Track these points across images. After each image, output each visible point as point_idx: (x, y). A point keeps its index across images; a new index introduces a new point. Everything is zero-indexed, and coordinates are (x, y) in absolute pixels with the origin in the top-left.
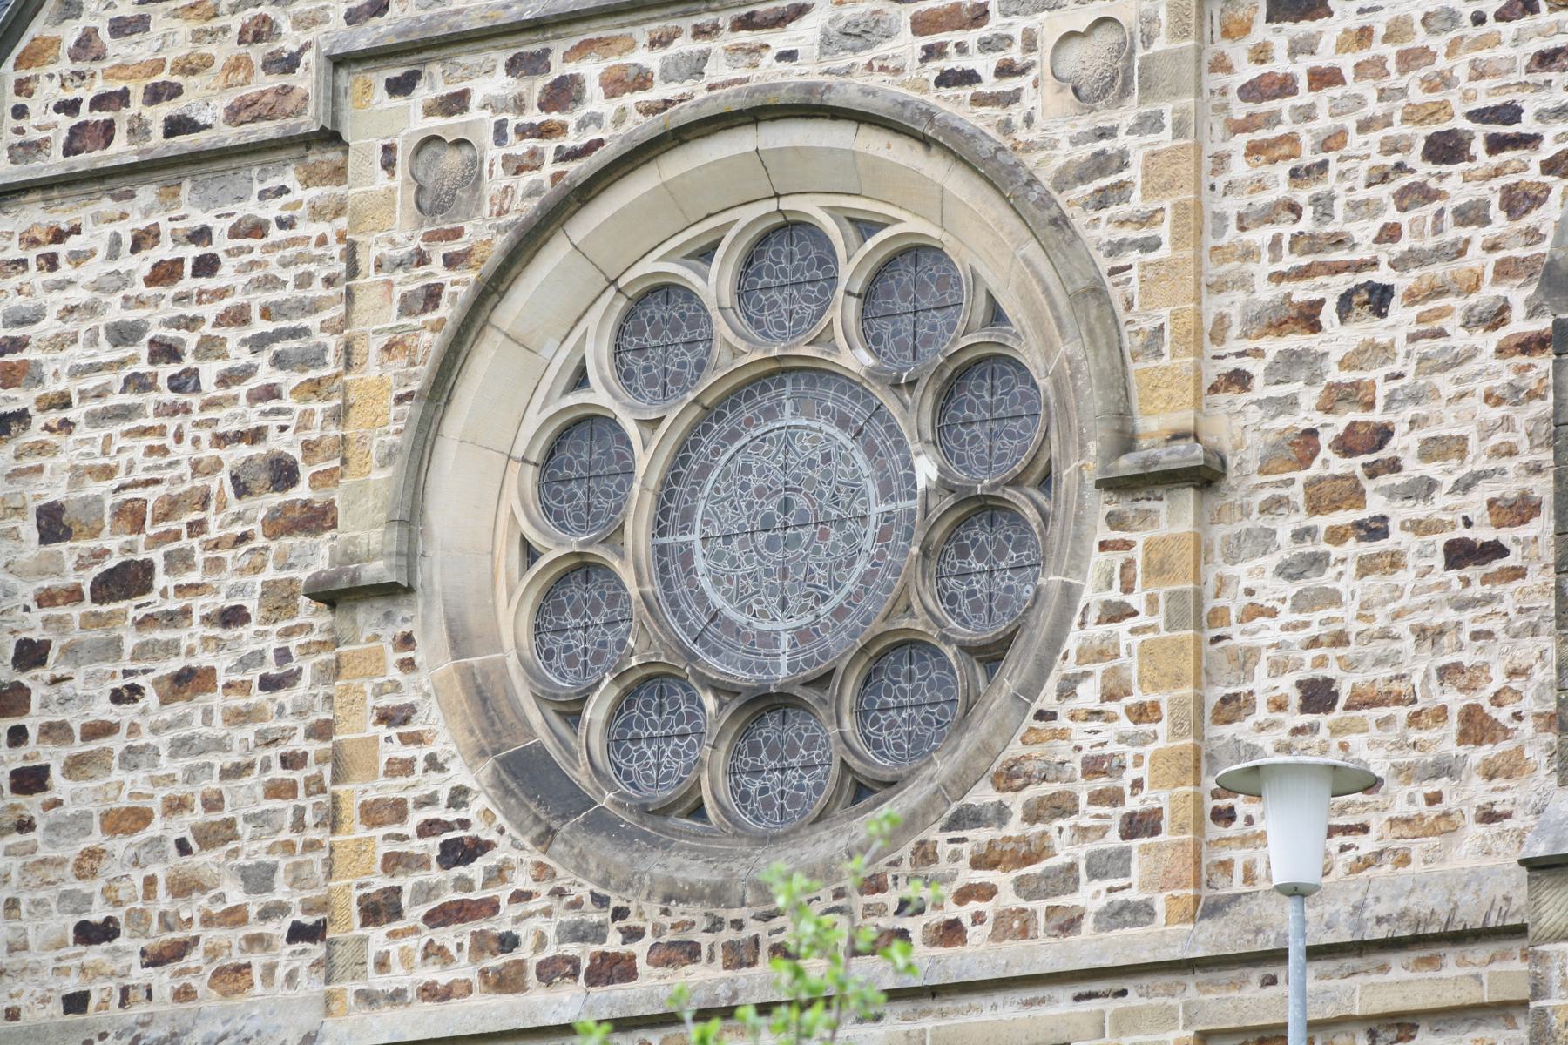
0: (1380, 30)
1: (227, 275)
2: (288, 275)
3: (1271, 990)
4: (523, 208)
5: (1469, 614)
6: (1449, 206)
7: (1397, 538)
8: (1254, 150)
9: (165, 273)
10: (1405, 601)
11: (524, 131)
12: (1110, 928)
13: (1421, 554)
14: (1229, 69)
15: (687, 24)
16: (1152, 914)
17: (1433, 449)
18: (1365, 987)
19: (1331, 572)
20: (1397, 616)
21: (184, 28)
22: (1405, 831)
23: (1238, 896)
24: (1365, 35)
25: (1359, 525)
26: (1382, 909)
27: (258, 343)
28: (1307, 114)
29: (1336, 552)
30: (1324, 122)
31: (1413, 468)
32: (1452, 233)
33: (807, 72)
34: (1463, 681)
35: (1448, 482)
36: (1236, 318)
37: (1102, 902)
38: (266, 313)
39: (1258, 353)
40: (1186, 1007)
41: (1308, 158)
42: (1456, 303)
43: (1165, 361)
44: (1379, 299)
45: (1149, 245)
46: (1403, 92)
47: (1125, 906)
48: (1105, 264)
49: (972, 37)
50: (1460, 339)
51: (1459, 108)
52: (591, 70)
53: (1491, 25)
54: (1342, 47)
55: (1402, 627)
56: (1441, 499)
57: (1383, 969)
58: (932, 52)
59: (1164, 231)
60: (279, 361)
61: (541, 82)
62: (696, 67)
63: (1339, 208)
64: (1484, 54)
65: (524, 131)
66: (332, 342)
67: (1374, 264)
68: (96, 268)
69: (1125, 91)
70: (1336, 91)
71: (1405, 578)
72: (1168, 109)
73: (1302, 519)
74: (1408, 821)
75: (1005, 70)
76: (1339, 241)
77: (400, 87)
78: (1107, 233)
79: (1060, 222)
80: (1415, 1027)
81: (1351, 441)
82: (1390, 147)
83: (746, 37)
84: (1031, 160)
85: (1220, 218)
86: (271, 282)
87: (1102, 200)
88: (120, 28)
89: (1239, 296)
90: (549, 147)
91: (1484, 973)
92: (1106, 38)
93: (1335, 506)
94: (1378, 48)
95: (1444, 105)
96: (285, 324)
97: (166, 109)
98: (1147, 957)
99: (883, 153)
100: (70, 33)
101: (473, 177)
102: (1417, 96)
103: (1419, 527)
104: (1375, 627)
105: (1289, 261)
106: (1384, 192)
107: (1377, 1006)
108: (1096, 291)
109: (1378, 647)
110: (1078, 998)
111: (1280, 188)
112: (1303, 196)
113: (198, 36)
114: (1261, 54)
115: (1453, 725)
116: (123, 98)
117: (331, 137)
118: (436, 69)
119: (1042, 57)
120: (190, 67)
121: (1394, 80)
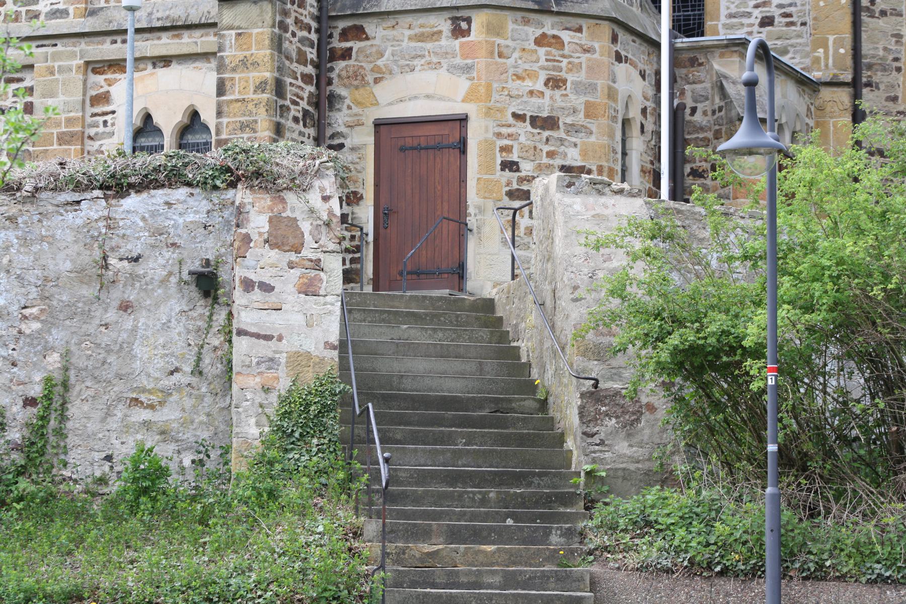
3: (114, 46)
12: (51, 19)
16: (68, 14)
18: (151, 45)
23: (102, 8)
26: (159, 15)
37: (48, 9)
40: (81, 51)
47: (58, 10)
57: (159, 38)
80: (171, 62)
91: (199, 41)
98: (65, 31)
110: (38, 47)
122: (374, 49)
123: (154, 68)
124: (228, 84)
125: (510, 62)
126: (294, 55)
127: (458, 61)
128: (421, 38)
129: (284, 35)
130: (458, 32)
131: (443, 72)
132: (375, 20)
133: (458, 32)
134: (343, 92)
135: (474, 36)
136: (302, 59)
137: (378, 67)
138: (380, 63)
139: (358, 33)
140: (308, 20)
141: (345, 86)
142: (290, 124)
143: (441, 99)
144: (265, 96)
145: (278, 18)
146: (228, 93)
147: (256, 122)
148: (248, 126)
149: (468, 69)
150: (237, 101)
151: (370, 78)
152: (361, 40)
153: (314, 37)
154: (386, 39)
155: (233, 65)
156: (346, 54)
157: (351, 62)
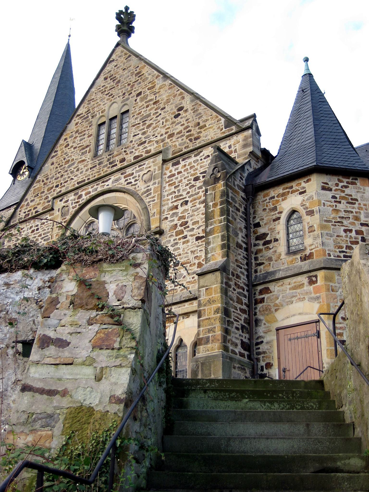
0: (187, 164)
1: (40, 230)
2: (46, 229)
4: (73, 213)
5: (199, 247)
6: (197, 187)
7: (189, 238)
8: (169, 185)
9: (33, 231)
10: (189, 247)
11: (75, 203)
13: (192, 240)
14: (166, 174)
15: (95, 184)
17: (194, 224)
19: (179, 245)
20: (188, 250)
21: (38, 199)
22: (189, 283)
24: (185, 165)
25: (183, 237)
26: (184, 296)
27: (42, 239)
28: (177, 178)
29: (179, 241)
30: (179, 179)
31: (191, 227)
32: (197, 191)
33: (110, 186)
34: (198, 258)
35: (196, 228)
36: (166, 210)
38: (44, 234)
39: (169, 214)
41: (177, 184)
42: (198, 201)
43: (155, 217)
44: (186, 202)
45: (154, 200)
46: (190, 172)
48: (147, 204)
49: (131, 177)
50: (198, 206)
51: (198, 173)
52: (83, 193)
53: (203, 160)
54: (182, 168)
55: (189, 252)
56: (195, 231)
57: (184, 306)
58: (126, 180)
59: (156, 198)
60: (44, 240)
61: (77, 196)
62: (96, 189)
63: (181, 191)
64: (202, 164)
65: (75, 203)
66: (50, 236)
67: (186, 198)
68: (26, 232)
69: (151, 180)
70: (181, 174)
71: (189, 244)
72: (157, 181)
73: (175, 237)
74: (189, 282)
75: (136, 181)
76: (181, 195)
77: (61, 201)
78: (148, 200)
79: (142, 199)
81: (182, 224)
82: (188, 180)
83: (103, 184)
84: (138, 192)
85: (164, 196)
86: (45, 230)
87: (147, 196)
88: (31, 201)
89: (167, 206)
90: (78, 204)
92: (149, 173)
93: (180, 235)
94: (187, 167)
95: (196, 173)
96: (46, 235)
97: (35, 210)
99: (119, 196)
100: (26, 203)
101: (69, 210)
102: (192, 172)
103: (191, 236)
104: (185, 252)
105: (174, 200)
106: (188, 187)
107: (183, 312)
108: (146, 208)
109: (185, 255)
111: (173, 190)
112: (176, 190)
113: (40, 200)
114: (171, 171)
115: (196, 265)
116: (31, 210)
117: (52, 209)
118: (65, 197)
119: (140, 178)
120: (38, 204)
121: (189, 171)
122: (274, 296)
123: (183, 319)
124: (203, 312)
125: (338, 293)
126: (235, 299)
127: (313, 295)
128: (295, 288)
129: (229, 289)
130: (312, 282)
131: (306, 301)
132: (274, 283)
133: (312, 282)
134: (261, 317)
135: (319, 283)
136: (240, 302)
137: (276, 304)
138: (277, 302)
139: (267, 290)
140: (242, 285)
141: (262, 315)
142: (233, 330)
143: (306, 314)
144: (219, 315)
145: (224, 280)
146: (202, 316)
147: (215, 327)
148: (211, 330)
149: (318, 298)
150: (207, 319)
151: (273, 310)
152: (268, 293)
153: (246, 293)
154: (279, 291)
155: (205, 303)
156: (262, 300)
157: (265, 304)
